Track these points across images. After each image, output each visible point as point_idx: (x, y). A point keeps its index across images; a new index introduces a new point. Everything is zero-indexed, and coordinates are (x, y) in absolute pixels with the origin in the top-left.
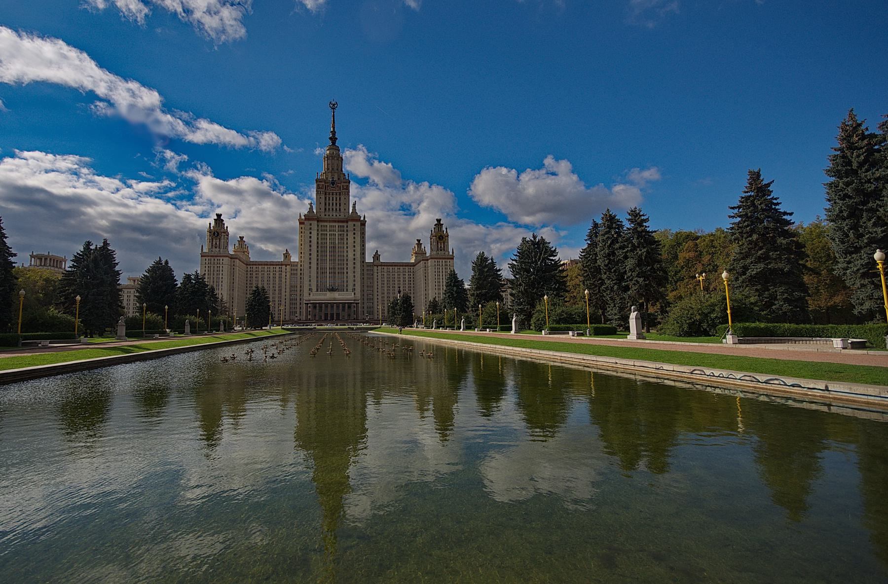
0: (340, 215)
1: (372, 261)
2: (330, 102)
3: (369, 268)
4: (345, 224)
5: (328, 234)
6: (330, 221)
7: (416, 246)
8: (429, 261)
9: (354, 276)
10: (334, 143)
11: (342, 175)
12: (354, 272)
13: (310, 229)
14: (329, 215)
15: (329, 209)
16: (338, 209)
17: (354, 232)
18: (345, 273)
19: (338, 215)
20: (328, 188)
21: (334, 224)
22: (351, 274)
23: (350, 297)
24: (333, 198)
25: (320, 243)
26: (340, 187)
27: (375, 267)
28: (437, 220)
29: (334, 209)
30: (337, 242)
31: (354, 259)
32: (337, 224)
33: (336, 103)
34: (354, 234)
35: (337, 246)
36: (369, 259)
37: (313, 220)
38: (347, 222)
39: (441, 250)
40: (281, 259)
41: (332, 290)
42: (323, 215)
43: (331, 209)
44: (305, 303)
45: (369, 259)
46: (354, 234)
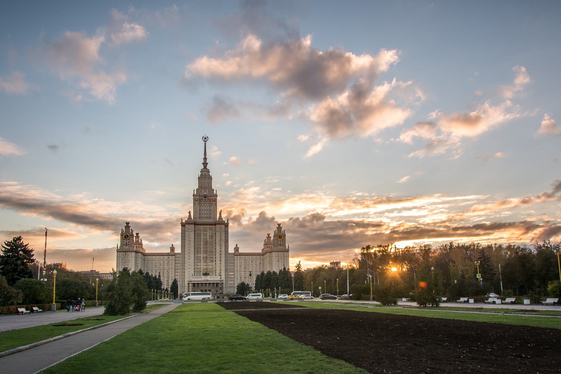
1: (234, 252)
2: (203, 137)
4: (214, 226)
5: (202, 233)
7: (266, 239)
8: (272, 253)
9: (221, 263)
10: (205, 167)
11: (211, 191)
12: (220, 261)
18: (214, 261)
20: (202, 200)
21: (206, 226)
22: (218, 262)
23: (218, 279)
26: (210, 200)
27: (236, 257)
30: (208, 239)
32: (208, 227)
33: (207, 137)
36: (231, 250)
37: (191, 224)
38: (215, 224)
39: (280, 246)
40: (168, 251)
41: (206, 274)
44: (188, 283)
45: (231, 250)
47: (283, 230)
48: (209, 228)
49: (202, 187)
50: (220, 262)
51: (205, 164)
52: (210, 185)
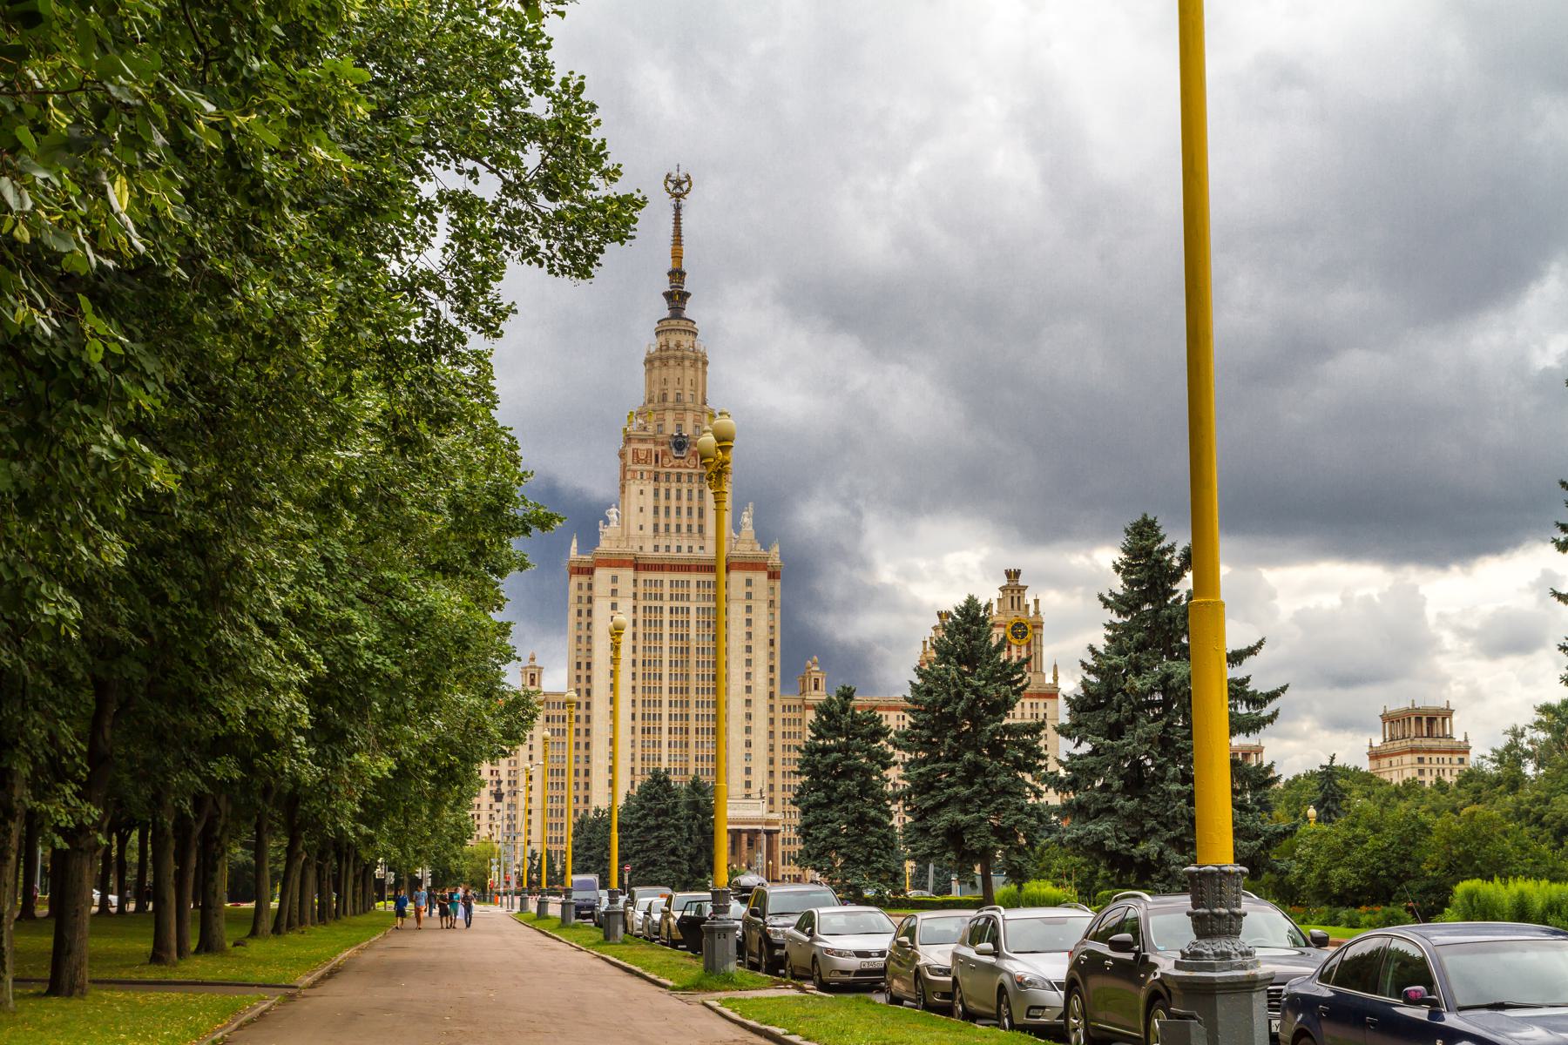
0: (702, 548)
2: (669, 176)
3: (791, 715)
6: (674, 568)
9: (748, 744)
12: (748, 730)
13: (614, 592)
14: (668, 548)
15: (667, 526)
16: (695, 529)
17: (749, 602)
19: (696, 549)
20: (666, 460)
24: (679, 491)
25: (640, 636)
28: (1008, 574)
29: (684, 529)
31: (748, 689)
32: (693, 578)
33: (688, 177)
34: (749, 609)
35: (693, 645)
42: (648, 550)
43: (673, 528)
46: (749, 609)
47: (1029, 599)
48: (698, 583)
49: (664, 398)
50: (745, 737)
51: (677, 298)
52: (700, 393)
